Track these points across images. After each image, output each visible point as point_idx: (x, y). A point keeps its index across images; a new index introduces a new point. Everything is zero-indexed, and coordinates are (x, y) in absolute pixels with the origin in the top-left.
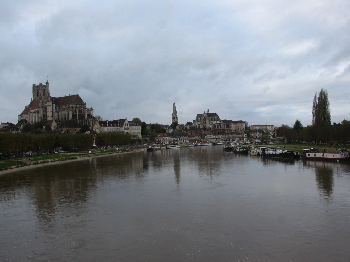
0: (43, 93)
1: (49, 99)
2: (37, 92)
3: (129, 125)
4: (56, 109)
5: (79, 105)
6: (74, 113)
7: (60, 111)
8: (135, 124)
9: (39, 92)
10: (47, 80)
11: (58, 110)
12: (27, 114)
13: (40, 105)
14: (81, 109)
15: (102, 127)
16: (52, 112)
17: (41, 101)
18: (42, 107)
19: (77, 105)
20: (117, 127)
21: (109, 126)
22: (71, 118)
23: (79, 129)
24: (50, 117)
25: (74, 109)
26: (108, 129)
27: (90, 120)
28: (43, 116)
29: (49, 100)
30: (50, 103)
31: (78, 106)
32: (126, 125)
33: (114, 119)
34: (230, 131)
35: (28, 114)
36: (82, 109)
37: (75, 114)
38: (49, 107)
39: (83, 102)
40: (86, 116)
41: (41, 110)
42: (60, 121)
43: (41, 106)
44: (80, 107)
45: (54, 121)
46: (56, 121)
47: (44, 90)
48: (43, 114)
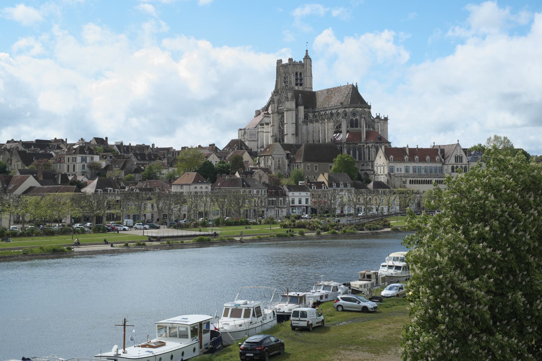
0: (297, 79)
2: (285, 78)
4: (306, 117)
5: (351, 109)
10: (307, 51)
14: (356, 120)
16: (294, 126)
19: (347, 110)
20: (433, 165)
21: (412, 160)
22: (330, 140)
24: (290, 135)
27: (370, 145)
29: (290, 97)
30: (291, 104)
33: (435, 145)
36: (358, 117)
38: (289, 112)
40: (364, 136)
44: (354, 114)
47: (299, 74)
48: (280, 128)
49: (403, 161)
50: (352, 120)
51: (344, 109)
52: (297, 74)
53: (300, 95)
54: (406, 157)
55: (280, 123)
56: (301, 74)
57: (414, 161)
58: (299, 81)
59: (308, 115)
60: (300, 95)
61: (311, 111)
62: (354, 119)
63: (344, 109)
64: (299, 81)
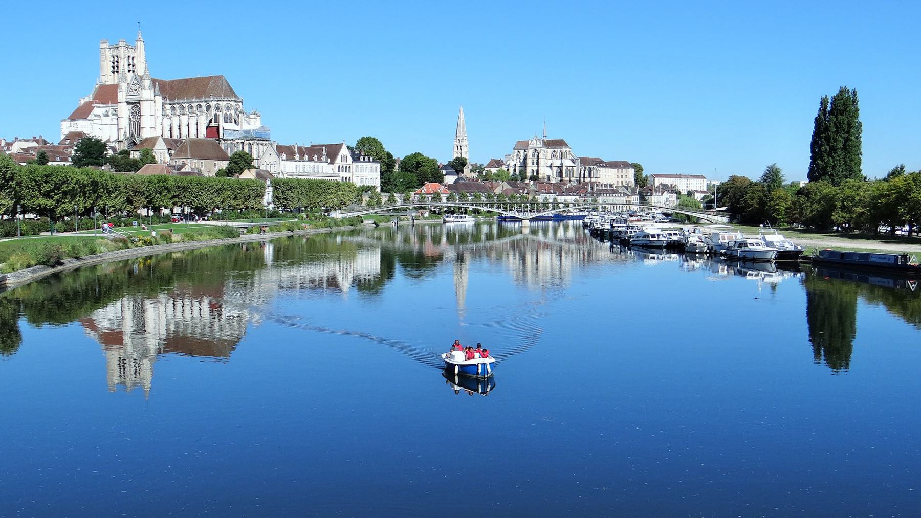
0: (129, 65)
1: (147, 83)
2: (113, 63)
3: (350, 159)
5: (225, 103)
6: (211, 121)
7: (175, 115)
8: (367, 158)
9: (117, 62)
11: (169, 112)
12: (86, 119)
13: (122, 96)
15: (283, 160)
17: (124, 86)
18: (128, 103)
21: (301, 159)
23: (224, 165)
25: (213, 111)
26: (297, 166)
28: (130, 124)
31: (223, 104)
32: (344, 158)
34: (597, 185)
35: (88, 118)
37: (213, 124)
39: (236, 96)
41: (125, 111)
42: (176, 141)
43: (125, 100)
45: (160, 141)
46: (165, 140)
48: (130, 119)
49: (294, 160)
50: (226, 114)
51: (217, 103)
52: (129, 57)
53: (157, 84)
54: (297, 157)
55: (130, 114)
56: (133, 58)
57: (304, 161)
58: (131, 66)
59: (165, 107)
60: (157, 84)
61: (168, 102)
62: (228, 113)
63: (217, 103)
64: (131, 66)
